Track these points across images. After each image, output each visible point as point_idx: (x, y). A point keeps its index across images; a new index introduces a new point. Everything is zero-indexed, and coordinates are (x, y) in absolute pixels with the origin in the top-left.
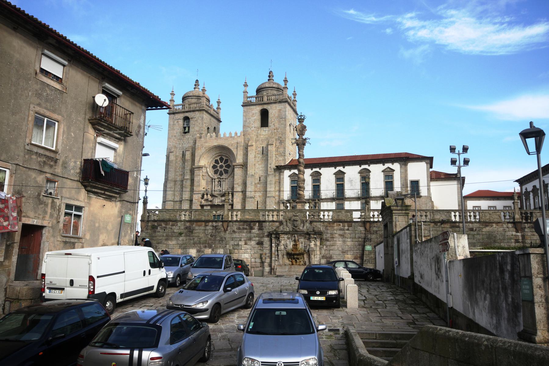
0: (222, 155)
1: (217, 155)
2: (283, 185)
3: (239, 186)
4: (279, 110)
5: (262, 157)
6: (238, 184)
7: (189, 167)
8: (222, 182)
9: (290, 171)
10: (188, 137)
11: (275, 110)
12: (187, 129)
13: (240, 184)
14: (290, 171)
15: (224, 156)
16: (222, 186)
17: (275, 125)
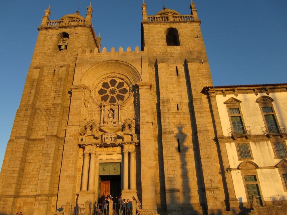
0: (114, 77)
1: (106, 76)
2: (218, 115)
3: (148, 114)
4: (191, 30)
5: (177, 78)
6: (146, 111)
7: (63, 87)
8: (116, 111)
9: (225, 96)
10: (64, 54)
11: (186, 30)
12: (63, 47)
13: (150, 111)
14: (225, 96)
15: (118, 78)
16: (116, 116)
17: (189, 44)
